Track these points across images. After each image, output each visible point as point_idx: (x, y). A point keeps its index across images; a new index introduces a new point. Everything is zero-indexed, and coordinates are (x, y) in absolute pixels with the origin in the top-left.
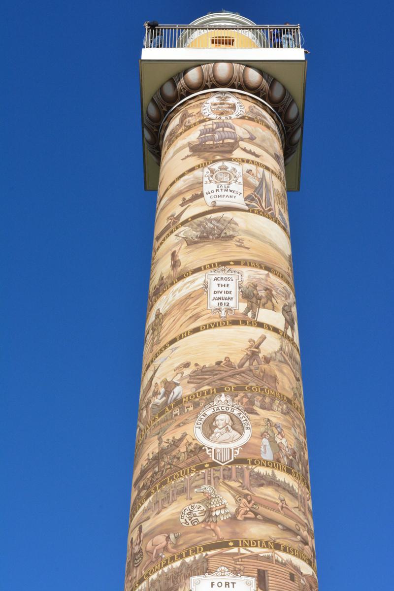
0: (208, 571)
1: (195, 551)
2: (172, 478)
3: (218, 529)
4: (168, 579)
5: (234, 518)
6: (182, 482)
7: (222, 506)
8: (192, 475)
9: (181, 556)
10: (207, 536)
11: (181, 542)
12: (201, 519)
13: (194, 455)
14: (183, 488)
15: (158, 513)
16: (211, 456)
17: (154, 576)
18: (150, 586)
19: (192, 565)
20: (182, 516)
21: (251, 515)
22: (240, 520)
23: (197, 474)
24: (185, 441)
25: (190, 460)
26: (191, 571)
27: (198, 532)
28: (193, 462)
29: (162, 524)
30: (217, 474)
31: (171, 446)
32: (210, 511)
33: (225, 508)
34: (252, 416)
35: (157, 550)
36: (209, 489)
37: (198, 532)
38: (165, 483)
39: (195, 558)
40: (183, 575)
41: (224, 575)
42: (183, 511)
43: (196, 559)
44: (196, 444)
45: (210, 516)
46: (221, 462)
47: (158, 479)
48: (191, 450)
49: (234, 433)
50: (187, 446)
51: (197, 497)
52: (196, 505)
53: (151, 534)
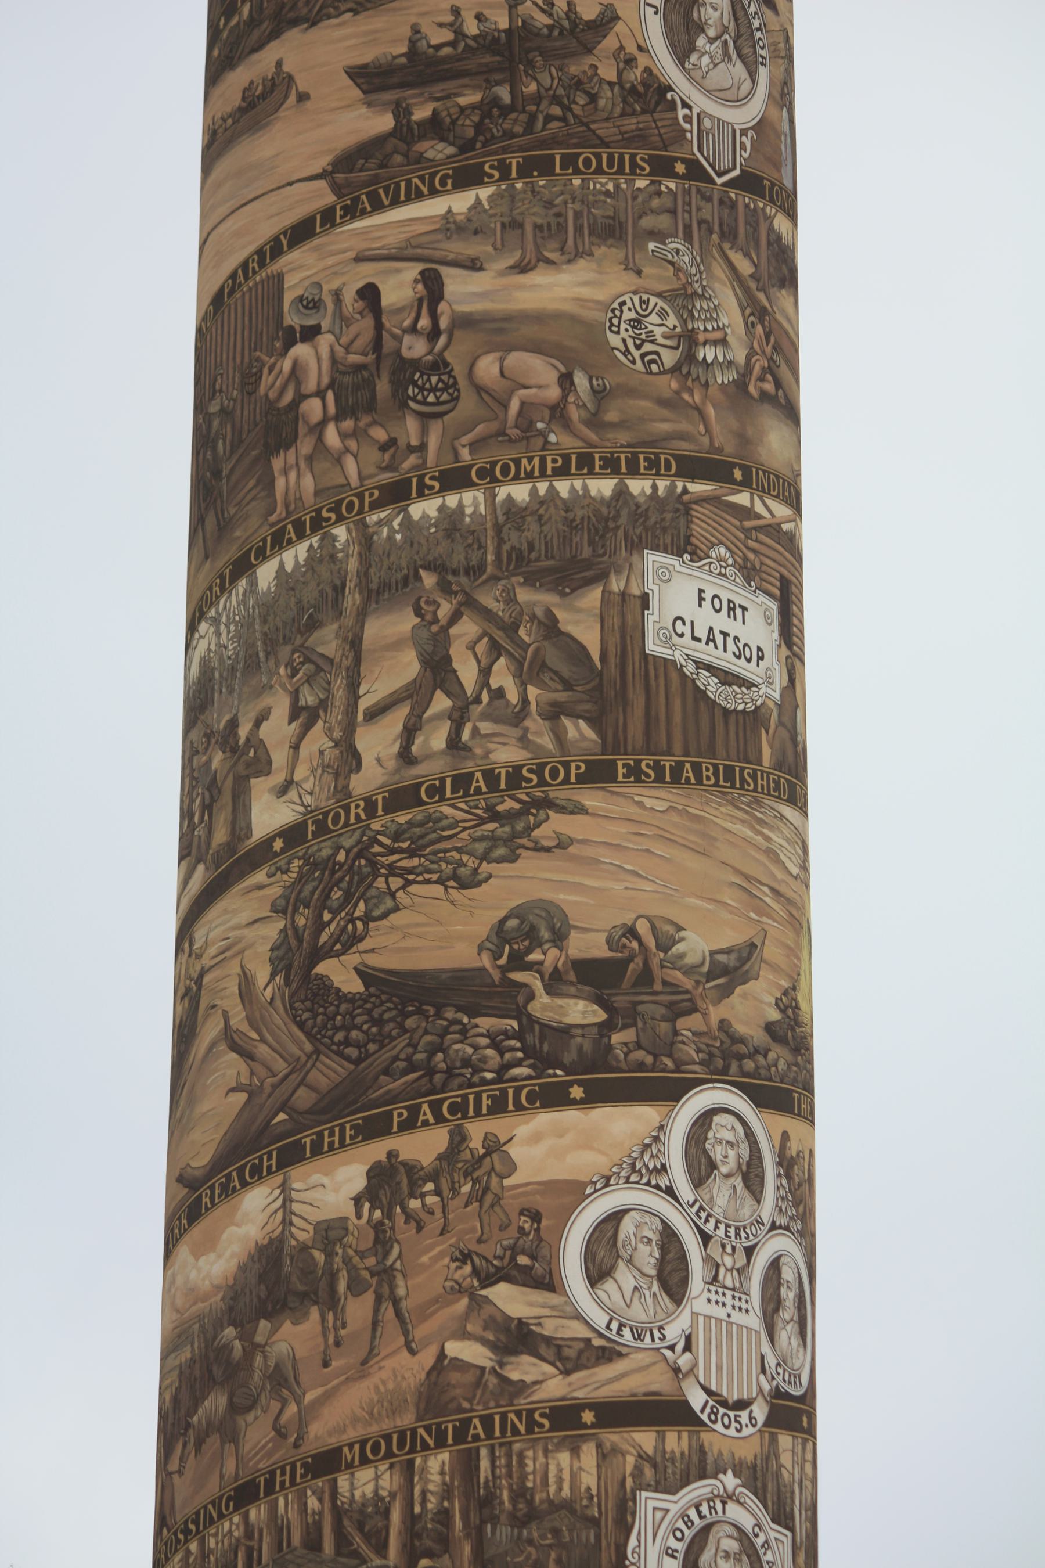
0: (689, 548)
1: (653, 465)
2: (569, 161)
3: (711, 411)
4: (570, 523)
5: (741, 384)
6: (607, 193)
7: (718, 335)
8: (641, 183)
9: (611, 466)
10: (684, 426)
11: (612, 416)
12: (669, 358)
13: (644, 112)
14: (613, 218)
15: (522, 268)
16: (689, 135)
17: (520, 492)
18: (501, 519)
19: (647, 510)
20: (612, 325)
21: (769, 387)
22: (752, 397)
23: (652, 188)
24: (610, 43)
25: (631, 124)
26: (646, 529)
27: (662, 402)
28: (638, 139)
29: (539, 318)
30: (706, 213)
31: (561, 33)
32: (688, 340)
33: (723, 342)
34: (768, 13)
35: (523, 404)
36: (686, 259)
37: (662, 402)
38: (545, 167)
39: (655, 487)
40: (620, 533)
41: (725, 575)
42: (616, 305)
43: (660, 493)
44: (648, 70)
45: (690, 357)
46: (713, 168)
47: (514, 136)
48: (633, 86)
49: (739, 70)
50: (621, 65)
51: (658, 277)
52: (653, 300)
53: (499, 330)
